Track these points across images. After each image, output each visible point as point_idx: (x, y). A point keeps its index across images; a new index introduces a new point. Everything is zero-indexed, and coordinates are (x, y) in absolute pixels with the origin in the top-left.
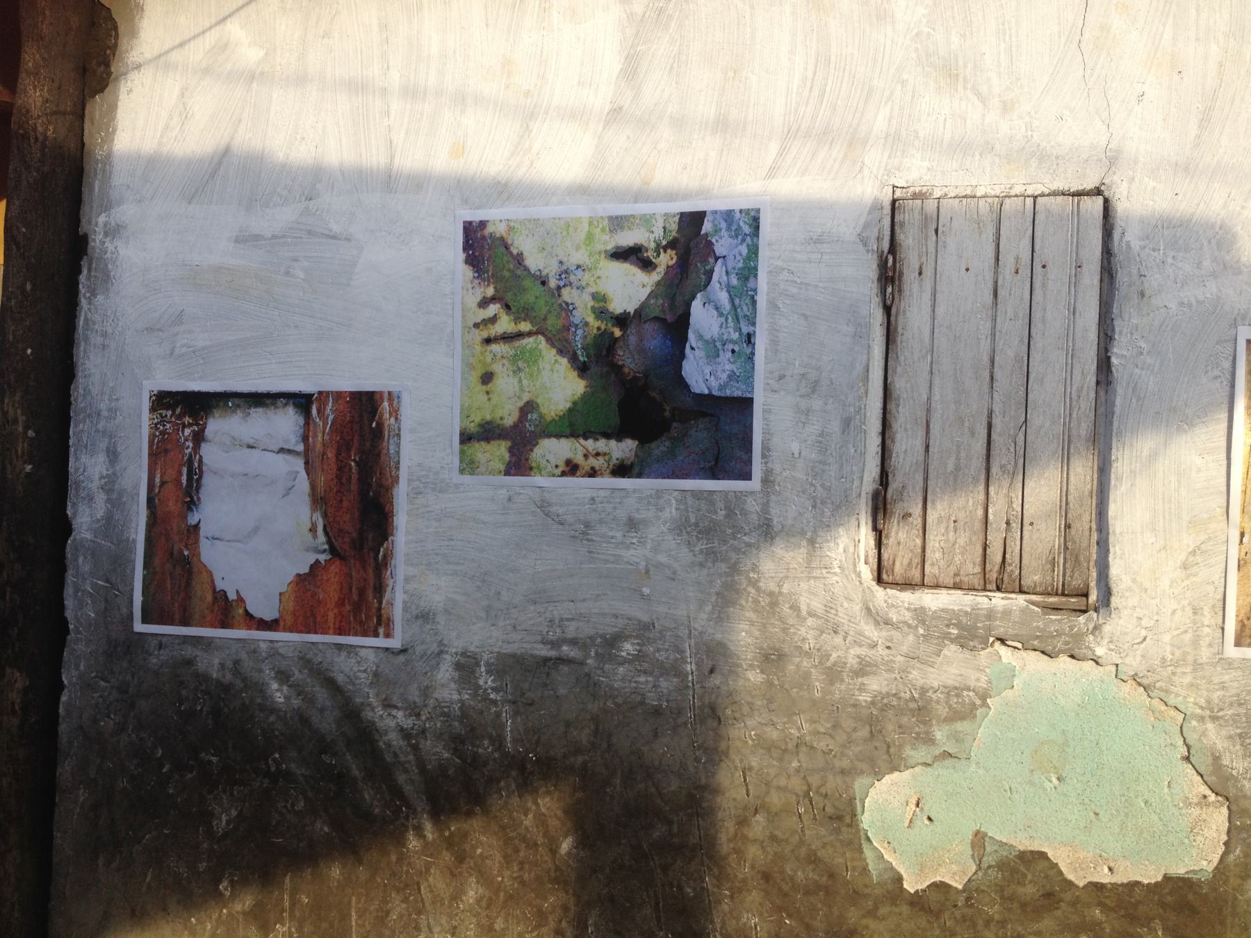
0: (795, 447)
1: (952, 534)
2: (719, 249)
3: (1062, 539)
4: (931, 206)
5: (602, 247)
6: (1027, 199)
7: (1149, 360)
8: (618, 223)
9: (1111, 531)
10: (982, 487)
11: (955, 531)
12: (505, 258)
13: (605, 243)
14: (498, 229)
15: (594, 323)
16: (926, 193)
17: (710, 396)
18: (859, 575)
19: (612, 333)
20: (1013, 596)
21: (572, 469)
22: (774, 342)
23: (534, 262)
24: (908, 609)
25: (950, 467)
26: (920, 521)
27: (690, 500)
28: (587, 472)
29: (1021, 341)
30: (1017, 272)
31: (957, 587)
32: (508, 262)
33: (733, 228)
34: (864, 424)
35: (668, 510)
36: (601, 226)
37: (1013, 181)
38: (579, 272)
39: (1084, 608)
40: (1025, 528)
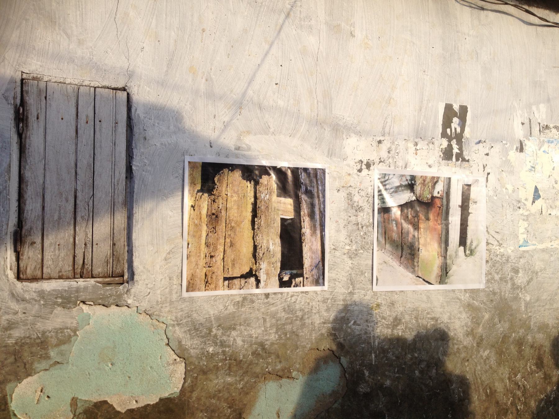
1: (57, 251)
3: (111, 251)
4: (42, 85)
6: (91, 88)
7: (149, 168)
9: (134, 246)
10: (72, 227)
11: (59, 250)
16: (39, 78)
20: (88, 280)
25: (56, 217)
26: (40, 246)
29: (90, 156)
30: (87, 123)
31: (60, 278)
37: (84, 79)
39: (122, 282)
40: (94, 246)
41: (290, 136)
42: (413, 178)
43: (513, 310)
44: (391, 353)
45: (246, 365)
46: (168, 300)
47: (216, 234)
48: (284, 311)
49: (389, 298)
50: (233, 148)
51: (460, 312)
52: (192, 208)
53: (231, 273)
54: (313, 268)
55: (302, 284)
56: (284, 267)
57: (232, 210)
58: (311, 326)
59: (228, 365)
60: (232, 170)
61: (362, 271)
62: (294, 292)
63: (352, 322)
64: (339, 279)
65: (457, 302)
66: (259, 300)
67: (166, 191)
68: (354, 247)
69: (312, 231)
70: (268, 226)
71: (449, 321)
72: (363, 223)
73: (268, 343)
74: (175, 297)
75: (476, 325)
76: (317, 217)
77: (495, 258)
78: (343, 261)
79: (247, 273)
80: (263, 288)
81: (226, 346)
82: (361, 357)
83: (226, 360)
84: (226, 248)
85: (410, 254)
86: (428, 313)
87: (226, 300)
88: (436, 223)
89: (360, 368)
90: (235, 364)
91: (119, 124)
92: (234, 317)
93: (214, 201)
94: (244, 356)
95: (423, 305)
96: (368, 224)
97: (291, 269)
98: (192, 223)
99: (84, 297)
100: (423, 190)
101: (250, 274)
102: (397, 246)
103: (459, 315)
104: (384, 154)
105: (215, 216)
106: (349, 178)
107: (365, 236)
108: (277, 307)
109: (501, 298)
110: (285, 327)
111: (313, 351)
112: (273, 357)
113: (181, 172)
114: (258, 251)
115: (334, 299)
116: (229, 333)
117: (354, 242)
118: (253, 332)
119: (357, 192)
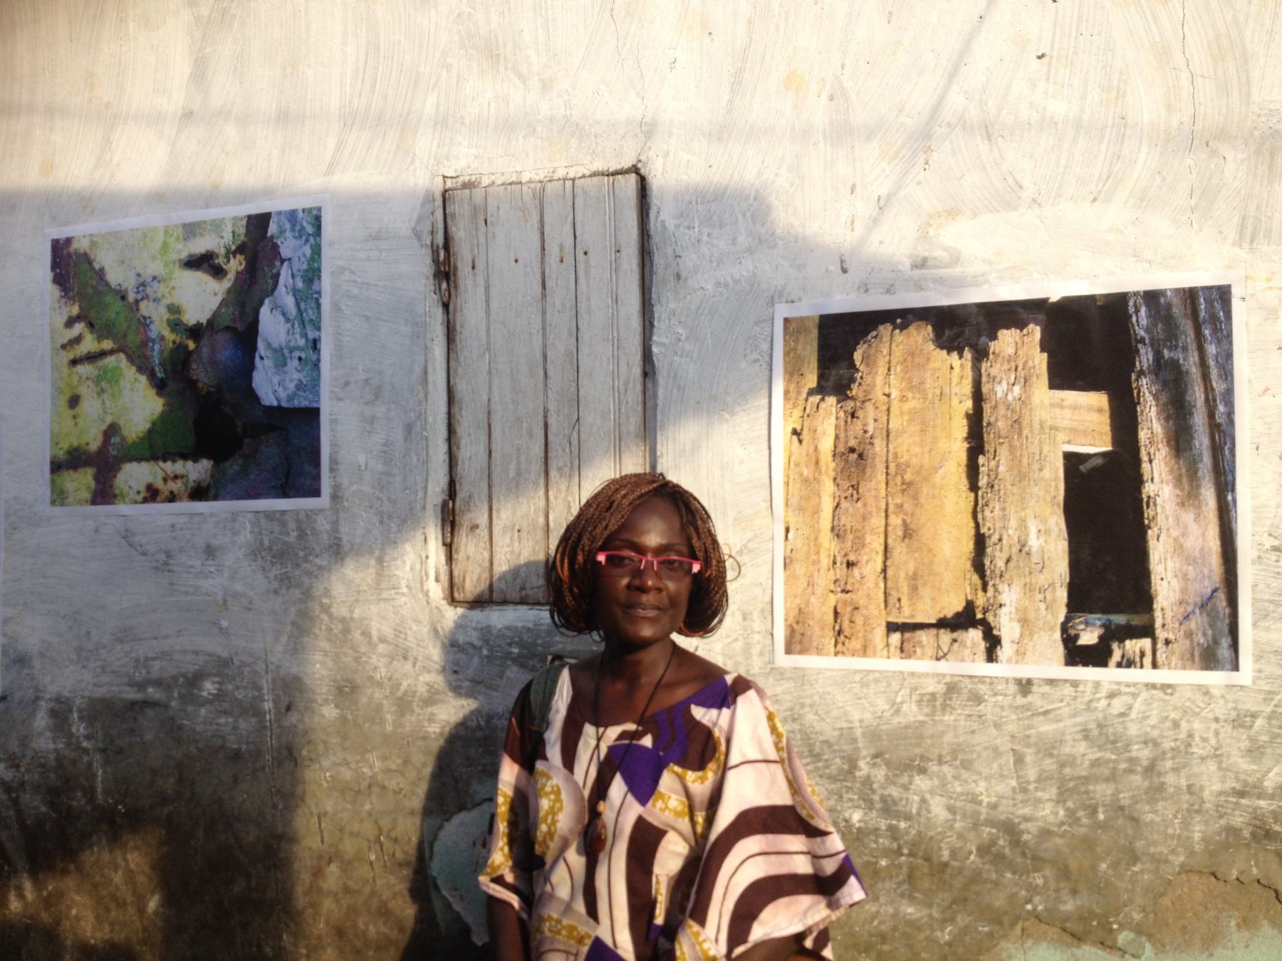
0: (362, 459)
1: (516, 544)
2: (285, 251)
4: (478, 194)
5: (175, 256)
6: (567, 182)
7: (688, 347)
8: (191, 230)
10: (541, 492)
11: (520, 542)
12: (89, 275)
13: (180, 251)
14: (81, 245)
15: (170, 336)
17: (279, 408)
18: (427, 594)
19: (187, 346)
21: (152, 494)
22: (339, 347)
23: (115, 276)
24: (475, 629)
25: (512, 473)
26: (485, 533)
27: (263, 521)
28: (167, 497)
29: (570, 334)
31: (523, 602)
32: (91, 278)
33: (298, 228)
34: (425, 430)
35: (243, 533)
36: (175, 234)
37: (555, 165)
38: (155, 284)
41: (1095, 200)
45: (961, 879)
47: (860, 504)
48: (1086, 738)
50: (907, 263)
52: (795, 438)
53: (906, 611)
54: (1190, 609)
55: (1148, 660)
57: (906, 436)
59: (905, 869)
60: (903, 327)
62: (1119, 683)
66: (1000, 698)
67: (729, 399)
69: (1182, 490)
73: (1031, 826)
76: (1202, 441)
79: (958, 615)
80: (1009, 661)
81: (898, 815)
83: (899, 852)
84: (890, 541)
87: (895, 686)
90: (926, 870)
91: (623, 253)
93: (853, 415)
94: (953, 853)
97: (1105, 611)
98: (796, 476)
99: (561, 646)
101: (965, 619)
105: (855, 456)
108: (1061, 725)
110: (1091, 788)
111: (1195, 878)
112: (1048, 872)
113: (765, 346)
114: (989, 550)
116: (905, 779)
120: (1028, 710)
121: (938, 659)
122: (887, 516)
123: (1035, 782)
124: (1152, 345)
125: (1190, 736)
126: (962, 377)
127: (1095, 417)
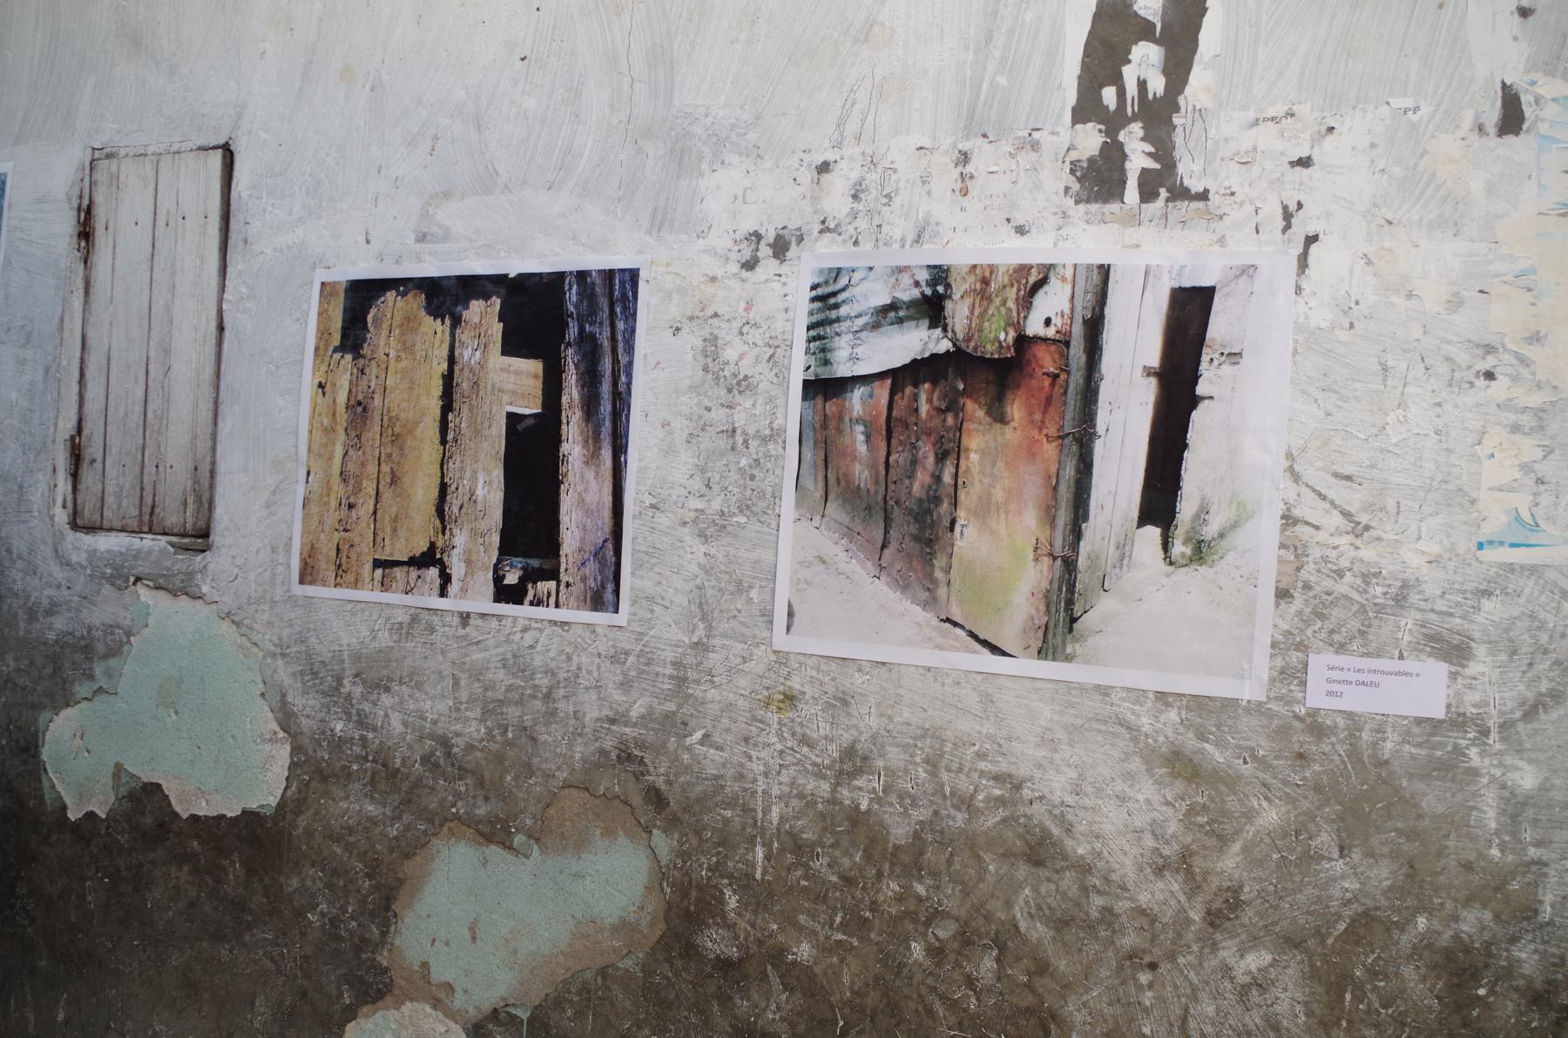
7: (248, 305)
26: (100, 466)
37: (172, 139)
41: (550, 188)
42: (940, 275)
43: (1420, 816)
44: (824, 861)
45: (407, 783)
46: (268, 596)
47: (360, 452)
48: (504, 666)
49: (833, 679)
51: (1129, 777)
52: (320, 390)
55: (552, 600)
56: (509, 546)
58: (572, 722)
59: (369, 774)
61: (739, 582)
63: (698, 735)
64: (663, 599)
65: (1115, 735)
68: (717, 504)
69: (588, 451)
70: (477, 433)
71: (1070, 800)
72: (751, 431)
73: (460, 741)
74: (279, 592)
75: (1211, 842)
76: (606, 407)
77: (1328, 584)
78: (679, 544)
79: (423, 553)
80: (455, 596)
81: (367, 727)
82: (719, 844)
83: (366, 759)
84: (381, 486)
85: (917, 538)
86: (981, 756)
88: (1035, 434)
89: (709, 879)
90: (383, 775)
92: (389, 661)
94: (403, 761)
95: (965, 726)
96: (768, 432)
97: (524, 557)
99: (141, 569)
100: (982, 315)
101: (429, 558)
102: (869, 508)
103: (1120, 786)
104: (836, 202)
106: (710, 289)
107: (755, 472)
108: (487, 654)
109: (1354, 754)
110: (505, 709)
112: (469, 781)
115: (647, 658)
116: (375, 696)
117: (716, 488)
118: (427, 707)
119: (736, 331)
120: (465, 640)
121: (407, 593)
122: (379, 464)
123: (466, 702)
124: (578, 320)
125: (579, 668)
126: (442, 342)
127: (531, 381)
